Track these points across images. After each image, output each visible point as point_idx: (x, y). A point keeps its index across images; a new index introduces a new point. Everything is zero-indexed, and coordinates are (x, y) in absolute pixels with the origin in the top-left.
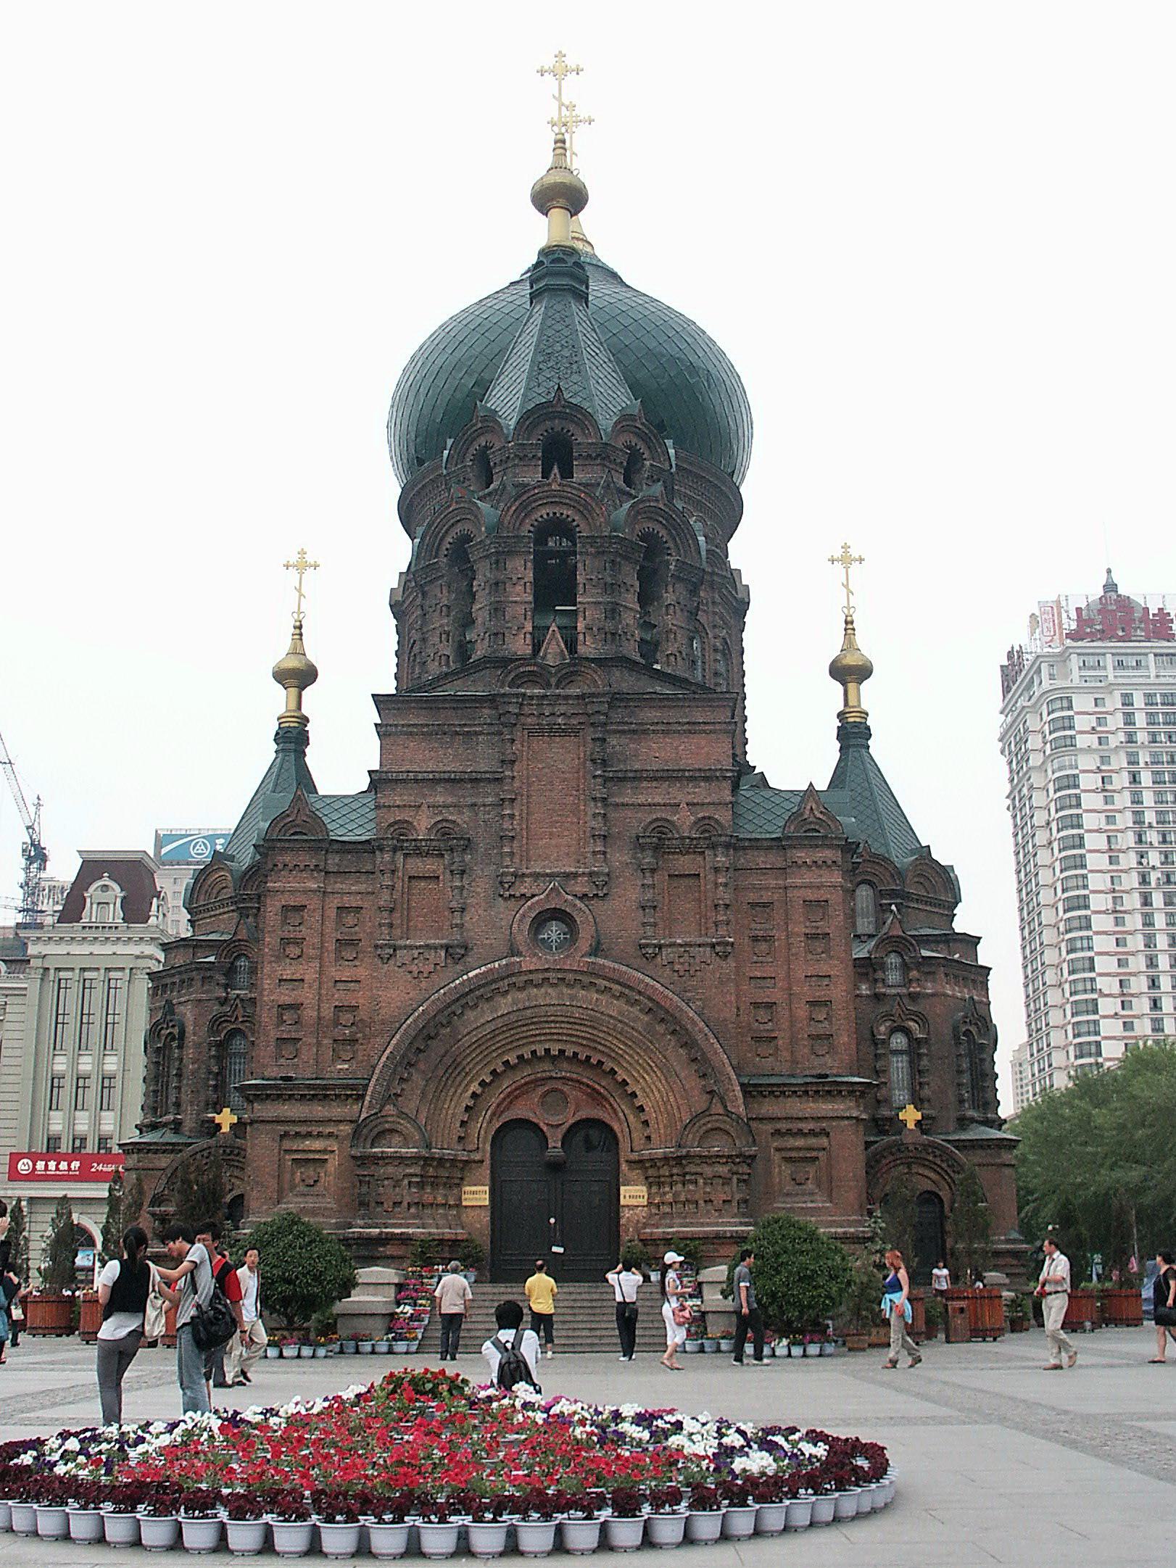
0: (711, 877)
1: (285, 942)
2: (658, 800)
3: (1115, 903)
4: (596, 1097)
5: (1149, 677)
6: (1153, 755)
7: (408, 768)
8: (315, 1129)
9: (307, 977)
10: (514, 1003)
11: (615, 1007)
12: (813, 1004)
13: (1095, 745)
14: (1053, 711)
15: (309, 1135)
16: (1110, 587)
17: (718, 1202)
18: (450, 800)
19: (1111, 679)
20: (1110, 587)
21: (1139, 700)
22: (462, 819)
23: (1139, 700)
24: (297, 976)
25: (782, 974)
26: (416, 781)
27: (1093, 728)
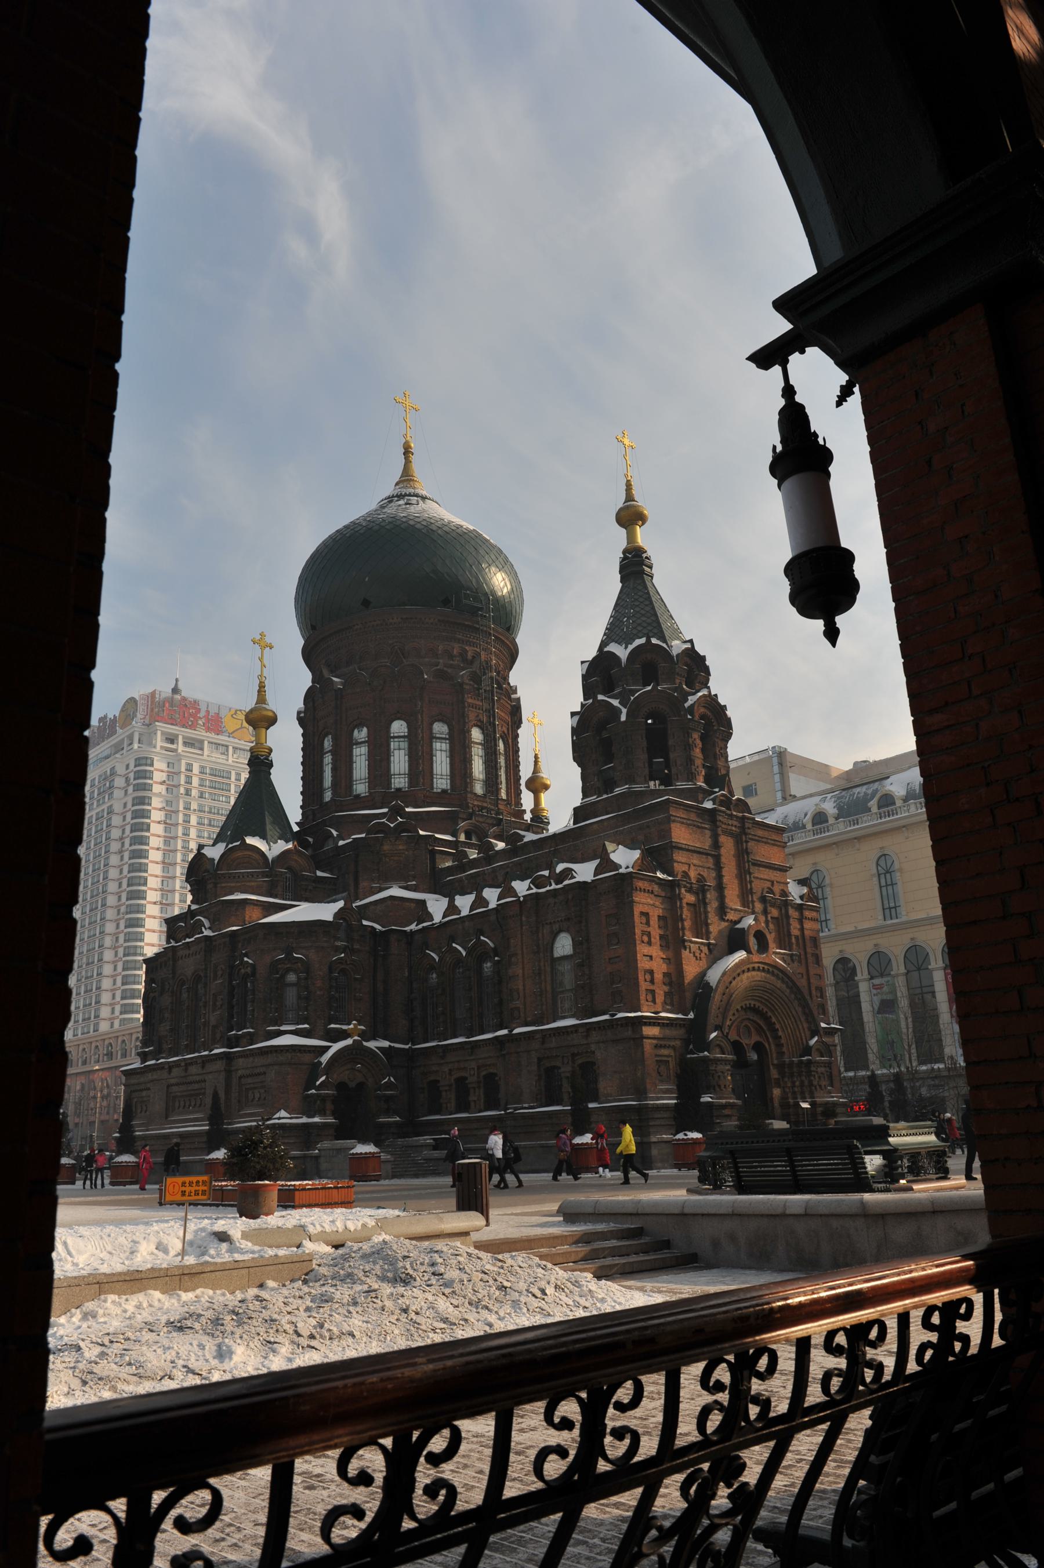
0: (785, 920)
1: (643, 933)
2: (766, 877)
3: (162, 898)
4: (759, 1030)
5: (202, 755)
6: (200, 805)
7: (685, 842)
8: (667, 1043)
9: (654, 955)
10: (748, 978)
11: (779, 984)
12: (817, 988)
13: (164, 792)
14: (139, 765)
15: (665, 1047)
16: (175, 690)
17: (823, 1087)
18: (701, 864)
19: (180, 751)
20: (175, 690)
21: (196, 769)
22: (705, 874)
23: (196, 769)
24: (650, 954)
25: (804, 973)
26: (688, 850)
27: (164, 782)
